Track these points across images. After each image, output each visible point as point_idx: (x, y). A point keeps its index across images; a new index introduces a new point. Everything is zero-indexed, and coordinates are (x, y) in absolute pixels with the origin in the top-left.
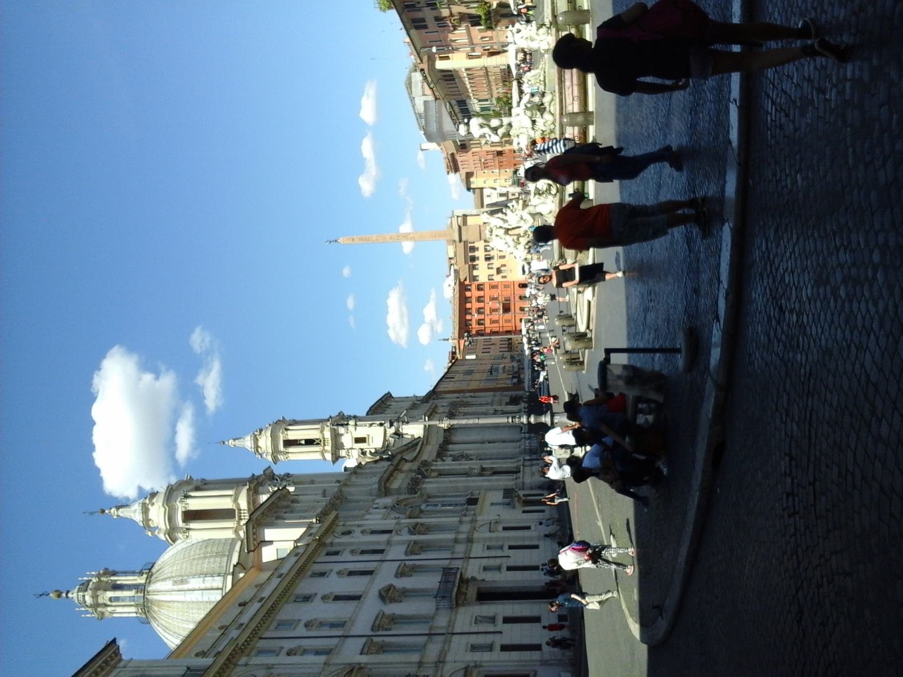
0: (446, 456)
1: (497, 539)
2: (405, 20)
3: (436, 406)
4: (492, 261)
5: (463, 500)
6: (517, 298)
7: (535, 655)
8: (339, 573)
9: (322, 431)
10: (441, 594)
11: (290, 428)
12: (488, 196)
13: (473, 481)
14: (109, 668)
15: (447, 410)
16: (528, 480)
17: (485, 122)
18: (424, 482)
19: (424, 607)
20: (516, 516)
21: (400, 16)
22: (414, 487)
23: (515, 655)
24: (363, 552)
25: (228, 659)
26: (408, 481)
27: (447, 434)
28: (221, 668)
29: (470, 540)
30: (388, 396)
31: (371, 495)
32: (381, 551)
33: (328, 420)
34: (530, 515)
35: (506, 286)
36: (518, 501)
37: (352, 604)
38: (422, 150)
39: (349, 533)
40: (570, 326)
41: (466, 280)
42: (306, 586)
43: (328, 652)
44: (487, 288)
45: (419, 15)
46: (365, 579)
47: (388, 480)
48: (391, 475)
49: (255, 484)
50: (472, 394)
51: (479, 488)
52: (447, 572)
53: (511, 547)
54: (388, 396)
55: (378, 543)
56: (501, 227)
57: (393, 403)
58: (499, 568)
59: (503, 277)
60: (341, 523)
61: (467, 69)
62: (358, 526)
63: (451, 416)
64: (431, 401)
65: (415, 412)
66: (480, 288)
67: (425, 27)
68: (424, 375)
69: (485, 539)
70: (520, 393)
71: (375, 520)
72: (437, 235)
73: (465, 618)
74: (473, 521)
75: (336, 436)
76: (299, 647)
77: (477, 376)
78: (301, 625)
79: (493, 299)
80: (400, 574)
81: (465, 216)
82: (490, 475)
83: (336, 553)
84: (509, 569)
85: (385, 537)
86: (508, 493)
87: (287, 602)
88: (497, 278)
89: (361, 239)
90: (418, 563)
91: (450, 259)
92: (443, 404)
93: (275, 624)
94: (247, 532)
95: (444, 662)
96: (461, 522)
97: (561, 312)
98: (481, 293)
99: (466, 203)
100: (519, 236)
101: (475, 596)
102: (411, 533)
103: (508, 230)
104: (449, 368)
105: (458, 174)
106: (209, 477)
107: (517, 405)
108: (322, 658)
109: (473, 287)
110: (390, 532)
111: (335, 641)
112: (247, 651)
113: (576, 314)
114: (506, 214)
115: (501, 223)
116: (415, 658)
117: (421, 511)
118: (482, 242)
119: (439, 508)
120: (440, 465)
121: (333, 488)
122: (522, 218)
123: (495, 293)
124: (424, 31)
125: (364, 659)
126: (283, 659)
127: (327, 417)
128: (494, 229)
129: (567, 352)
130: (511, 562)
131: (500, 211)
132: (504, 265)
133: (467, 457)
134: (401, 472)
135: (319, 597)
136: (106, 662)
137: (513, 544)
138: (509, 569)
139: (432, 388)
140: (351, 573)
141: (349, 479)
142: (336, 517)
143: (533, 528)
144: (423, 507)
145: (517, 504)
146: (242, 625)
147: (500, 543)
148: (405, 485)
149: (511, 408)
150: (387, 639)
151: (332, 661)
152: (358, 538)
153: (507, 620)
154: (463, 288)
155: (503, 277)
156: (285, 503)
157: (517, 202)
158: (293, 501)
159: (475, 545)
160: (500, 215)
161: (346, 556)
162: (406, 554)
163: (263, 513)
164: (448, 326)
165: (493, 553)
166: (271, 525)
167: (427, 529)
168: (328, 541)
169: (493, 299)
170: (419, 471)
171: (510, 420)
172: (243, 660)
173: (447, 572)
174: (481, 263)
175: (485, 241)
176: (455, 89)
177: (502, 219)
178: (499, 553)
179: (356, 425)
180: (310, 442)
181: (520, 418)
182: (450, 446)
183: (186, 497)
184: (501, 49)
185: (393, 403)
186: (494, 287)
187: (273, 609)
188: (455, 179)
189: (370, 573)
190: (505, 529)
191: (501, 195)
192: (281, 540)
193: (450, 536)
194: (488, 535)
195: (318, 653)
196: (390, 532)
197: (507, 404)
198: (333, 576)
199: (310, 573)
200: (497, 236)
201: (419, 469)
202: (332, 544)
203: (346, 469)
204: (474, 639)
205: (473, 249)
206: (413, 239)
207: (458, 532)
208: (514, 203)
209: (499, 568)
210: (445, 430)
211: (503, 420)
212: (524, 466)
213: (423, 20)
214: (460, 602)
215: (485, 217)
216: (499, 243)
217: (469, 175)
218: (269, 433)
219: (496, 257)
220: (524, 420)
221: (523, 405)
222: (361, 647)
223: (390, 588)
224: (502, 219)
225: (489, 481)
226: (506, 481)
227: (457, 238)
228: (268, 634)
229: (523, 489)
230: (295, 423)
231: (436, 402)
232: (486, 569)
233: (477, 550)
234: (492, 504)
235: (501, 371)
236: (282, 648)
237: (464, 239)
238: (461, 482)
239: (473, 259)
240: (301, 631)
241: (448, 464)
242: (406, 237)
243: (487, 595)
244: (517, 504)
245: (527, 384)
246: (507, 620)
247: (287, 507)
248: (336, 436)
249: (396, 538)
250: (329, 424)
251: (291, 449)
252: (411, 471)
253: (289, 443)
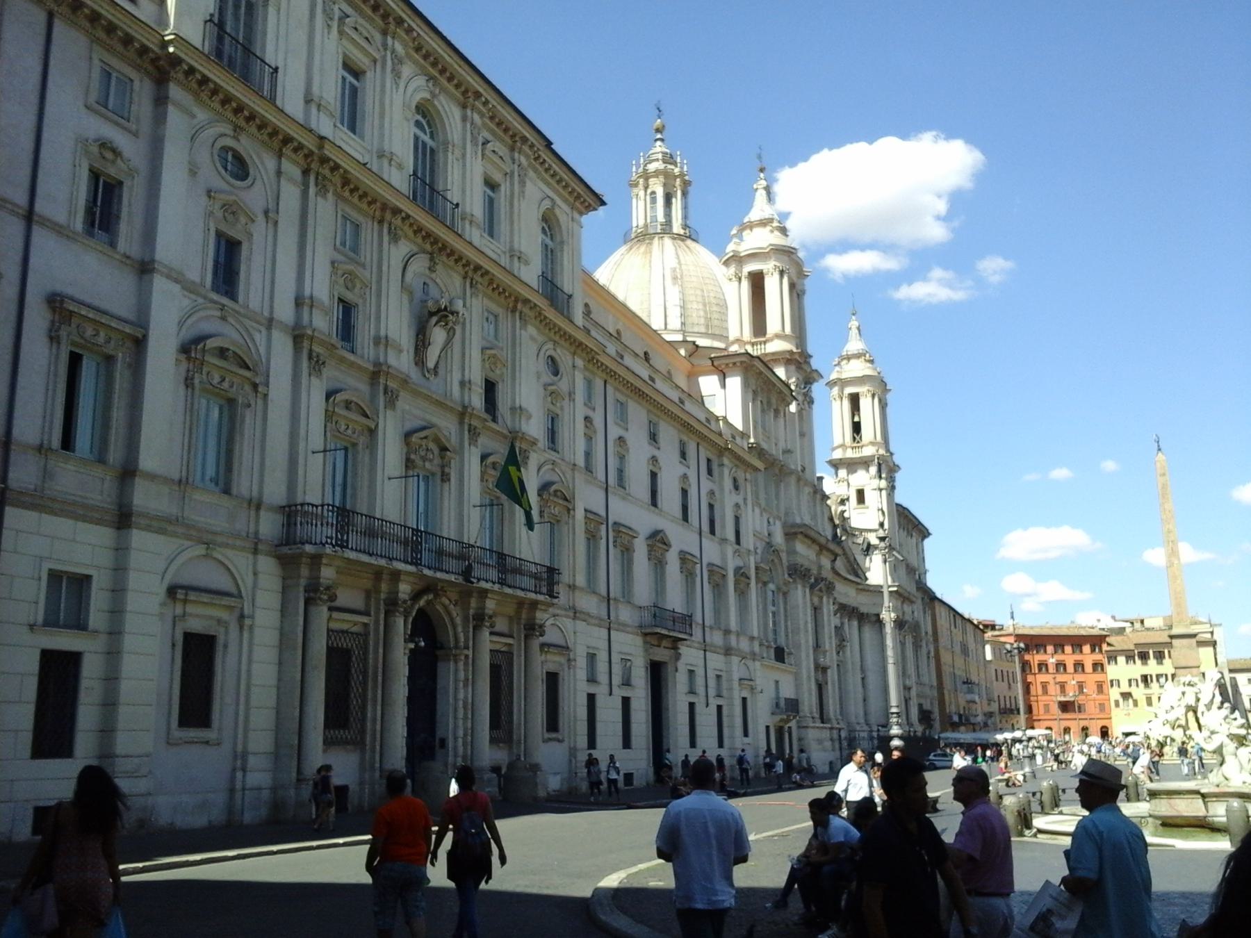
0: (841, 618)
1: (730, 689)
3: (912, 602)
4: (1141, 685)
5: (782, 641)
6: (1083, 723)
7: (582, 741)
8: (685, 477)
9: (872, 443)
10: (658, 612)
11: (876, 400)
13: (808, 656)
14: (571, 200)
16: (812, 735)
18: (804, 586)
19: (643, 591)
20: (762, 716)
22: (798, 572)
23: (582, 713)
24: (711, 507)
25: (581, 344)
26: (806, 564)
27: (874, 619)
28: (570, 336)
29: (728, 651)
30: (924, 533)
31: (786, 514)
32: (712, 532)
33: (888, 450)
34: (763, 736)
35: (1102, 707)
36: (782, 720)
37: (646, 496)
39: (736, 488)
40: (1041, 803)
41: (1109, 644)
42: (669, 435)
43: (589, 468)
44: (1098, 677)
46: (678, 513)
47: (806, 536)
48: (814, 541)
49: (799, 360)
50: (932, 654)
51: (798, 665)
52: (686, 620)
53: (719, 708)
54: (924, 533)
55: (723, 527)
56: (1198, 700)
57: (914, 540)
58: (692, 692)
59: (1117, 704)
60: (748, 476)
62: (745, 503)
63: (900, 624)
64: (919, 595)
65: (902, 571)
66: (1098, 666)
69: (729, 672)
70: (937, 725)
71: (753, 522)
72: (1179, 602)
73: (630, 646)
74: (754, 656)
75: (865, 463)
76: (595, 432)
77: (959, 662)
78: (621, 432)
79: (1081, 686)
80: (684, 557)
81: (1214, 644)
82: (817, 680)
83: (710, 472)
84: (692, 705)
85: (731, 536)
86: (793, 706)
87: (649, 411)
88: (1114, 694)
89: (1164, 487)
90: (698, 579)
91: (1142, 622)
92: (916, 611)
93: (622, 398)
94: (736, 355)
95: (575, 618)
96: (752, 638)
97: (1064, 791)
98: (1089, 668)
100: (1185, 728)
101: (656, 658)
102: (737, 570)
103: (1195, 712)
104: (970, 621)
106: (808, 300)
107: (920, 721)
108: (581, 462)
109: (1097, 657)
110: (738, 542)
111: (601, 477)
112: (591, 366)
113: (1061, 813)
114: (1219, 708)
116: (581, 580)
117: (765, 584)
118: (1173, 671)
119: (771, 608)
120: (828, 608)
121: (795, 463)
122: (1213, 733)
123: (1090, 689)
125: (580, 514)
126: (581, 411)
128: (1195, 689)
129: (1001, 797)
130: (699, 708)
131: (1225, 698)
132: (1136, 703)
133: (841, 647)
134: (819, 554)
135: (656, 453)
136: (578, 197)
137: (725, 712)
138: (692, 705)
139: (939, 595)
140: (685, 493)
141: (807, 483)
142: (756, 469)
143: (746, 740)
144: (771, 586)
145: (778, 718)
146: (622, 357)
147: (725, 693)
148: (800, 560)
149: (914, 712)
150: (603, 541)
151: (577, 475)
152: (729, 500)
153: (626, 701)
154: (1096, 641)
155: (1117, 704)
156: (774, 401)
157: (1242, 726)
158: (777, 412)
159: (722, 658)
160: (1218, 699)
161: (706, 485)
162: (709, 564)
163: (761, 373)
164: (1034, 620)
165: (712, 683)
166: (746, 385)
167: (742, 593)
168: (726, 461)
169: (1081, 686)
170: (819, 579)
172: (580, 363)
173: (686, 620)
174: (1137, 669)
175: (1173, 676)
177: (1212, 701)
178: (712, 692)
180: (857, 428)
182: (855, 623)
183: (782, 273)
185: (914, 540)
186: (1100, 687)
187: (640, 394)
189: (685, 517)
190: (744, 700)
192: (726, 400)
193: (733, 624)
194: (736, 677)
195: (588, 455)
196: (738, 542)
197: (920, 706)
198: (681, 470)
199: (685, 438)
200: (1183, 693)
201: (822, 579)
202: (721, 465)
203: (821, 479)
204: (602, 657)
205: (1160, 657)
206: (1170, 565)
207: (738, 634)
208: (1241, 721)
209: (692, 692)
210: (878, 615)
212: (831, 729)
214: (648, 638)
215: (1213, 675)
216: (1172, 697)
218: (869, 372)
219: (1148, 691)
221: (919, 729)
222: (594, 510)
223: (666, 544)
224: (1212, 701)
225: (809, 677)
226: (809, 703)
227: (1175, 631)
228: (610, 389)
229: (799, 727)
230: (883, 406)
231: (919, 601)
232: (691, 672)
233: (716, 661)
234: (777, 682)
235: (969, 697)
236: (594, 409)
237: (1175, 642)
238: (806, 640)
239: (1144, 657)
240: (614, 431)
241: (831, 620)
242: (1173, 553)
243: (657, 673)
244: (778, 718)
245: (951, 735)
246: (626, 701)
247: (769, 403)
248: (865, 463)
249: (730, 550)
250: (882, 452)
251: (846, 404)
252: (820, 567)
253: (855, 400)
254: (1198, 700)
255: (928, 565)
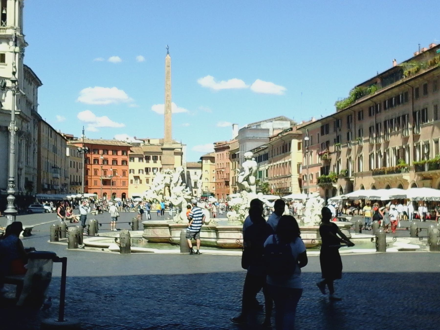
2: (328, 119)
3: (27, 121)
9: (12, 28)
12: (195, 173)
15: (23, 130)
17: (253, 172)
21: (331, 116)
30: (38, 83)
33: (21, 33)
38: (233, 125)
40: (88, 231)
45: (331, 130)
54: (38, 83)
56: (171, 181)
61: (290, 162)
63: (19, 133)
65: (24, 104)
67: (322, 134)
68: (52, 110)
70: (35, 190)
72: (168, 132)
81: (181, 154)
91: (149, 141)
92: (29, 127)
97: (101, 225)
99: (192, 156)
100: (163, 195)
103: (169, 187)
105: (214, 151)
107: (25, 187)
113: (98, 236)
114: (181, 185)
115: (174, 181)
118: (161, 166)
122: (178, 196)
124: (319, 132)
127: (24, 33)
128: (170, 176)
129: (67, 228)
131: (184, 181)
149: (23, 182)
157: (190, 195)
160: (181, 181)
164: (94, 136)
171: (11, 179)
175: (161, 169)
176: (276, 153)
177: (177, 182)
179: (15, 53)
181: (13, 187)
184: (303, 189)
188: (210, 149)
191: (195, 183)
205: (155, 159)
206: (166, 113)
208: (190, 192)
211: (11, 173)
213: (327, 132)
215: (179, 169)
216: (159, 179)
217: (212, 159)
220: (11, 191)
221: (25, 192)
224: (177, 182)
227: (165, 146)
230: (21, 7)
231: (32, 121)
237: (164, 152)
242: (168, 107)
245: (42, 195)
250: (18, 33)
254: (171, 181)
255: (39, 102)
